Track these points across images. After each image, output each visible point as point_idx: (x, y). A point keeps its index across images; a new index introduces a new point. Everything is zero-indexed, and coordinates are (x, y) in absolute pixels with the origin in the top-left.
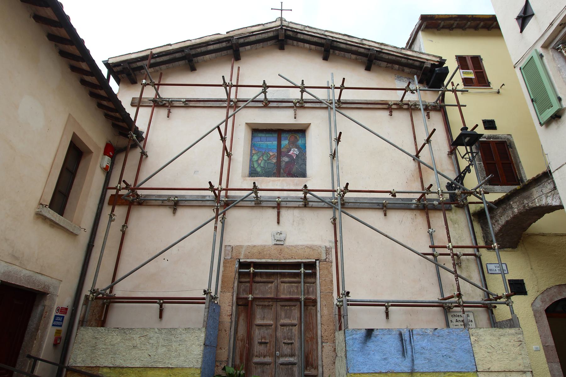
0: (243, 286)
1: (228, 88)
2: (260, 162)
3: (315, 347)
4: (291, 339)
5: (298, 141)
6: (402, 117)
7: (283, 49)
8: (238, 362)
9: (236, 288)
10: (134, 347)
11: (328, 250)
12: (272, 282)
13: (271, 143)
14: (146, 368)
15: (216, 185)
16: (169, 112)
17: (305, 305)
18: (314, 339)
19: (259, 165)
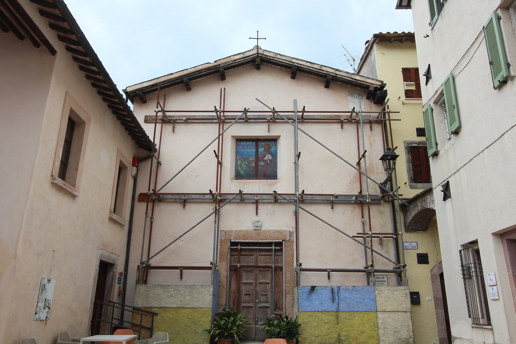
0: (233, 257)
1: (219, 113)
2: (242, 166)
3: (281, 297)
4: (266, 292)
5: (271, 148)
6: (350, 129)
7: (260, 69)
8: (232, 306)
9: (229, 259)
10: (171, 296)
11: (291, 233)
12: (253, 255)
13: (250, 150)
14: (179, 308)
15: (214, 192)
16: (174, 127)
17: (275, 270)
18: (281, 292)
19: (242, 168)
